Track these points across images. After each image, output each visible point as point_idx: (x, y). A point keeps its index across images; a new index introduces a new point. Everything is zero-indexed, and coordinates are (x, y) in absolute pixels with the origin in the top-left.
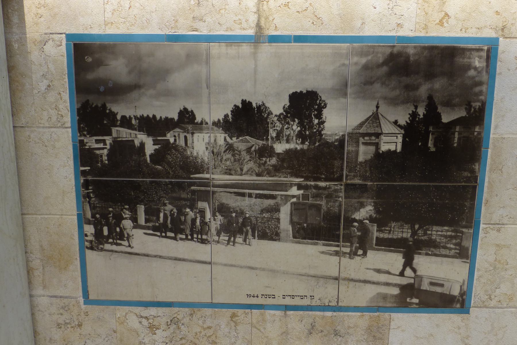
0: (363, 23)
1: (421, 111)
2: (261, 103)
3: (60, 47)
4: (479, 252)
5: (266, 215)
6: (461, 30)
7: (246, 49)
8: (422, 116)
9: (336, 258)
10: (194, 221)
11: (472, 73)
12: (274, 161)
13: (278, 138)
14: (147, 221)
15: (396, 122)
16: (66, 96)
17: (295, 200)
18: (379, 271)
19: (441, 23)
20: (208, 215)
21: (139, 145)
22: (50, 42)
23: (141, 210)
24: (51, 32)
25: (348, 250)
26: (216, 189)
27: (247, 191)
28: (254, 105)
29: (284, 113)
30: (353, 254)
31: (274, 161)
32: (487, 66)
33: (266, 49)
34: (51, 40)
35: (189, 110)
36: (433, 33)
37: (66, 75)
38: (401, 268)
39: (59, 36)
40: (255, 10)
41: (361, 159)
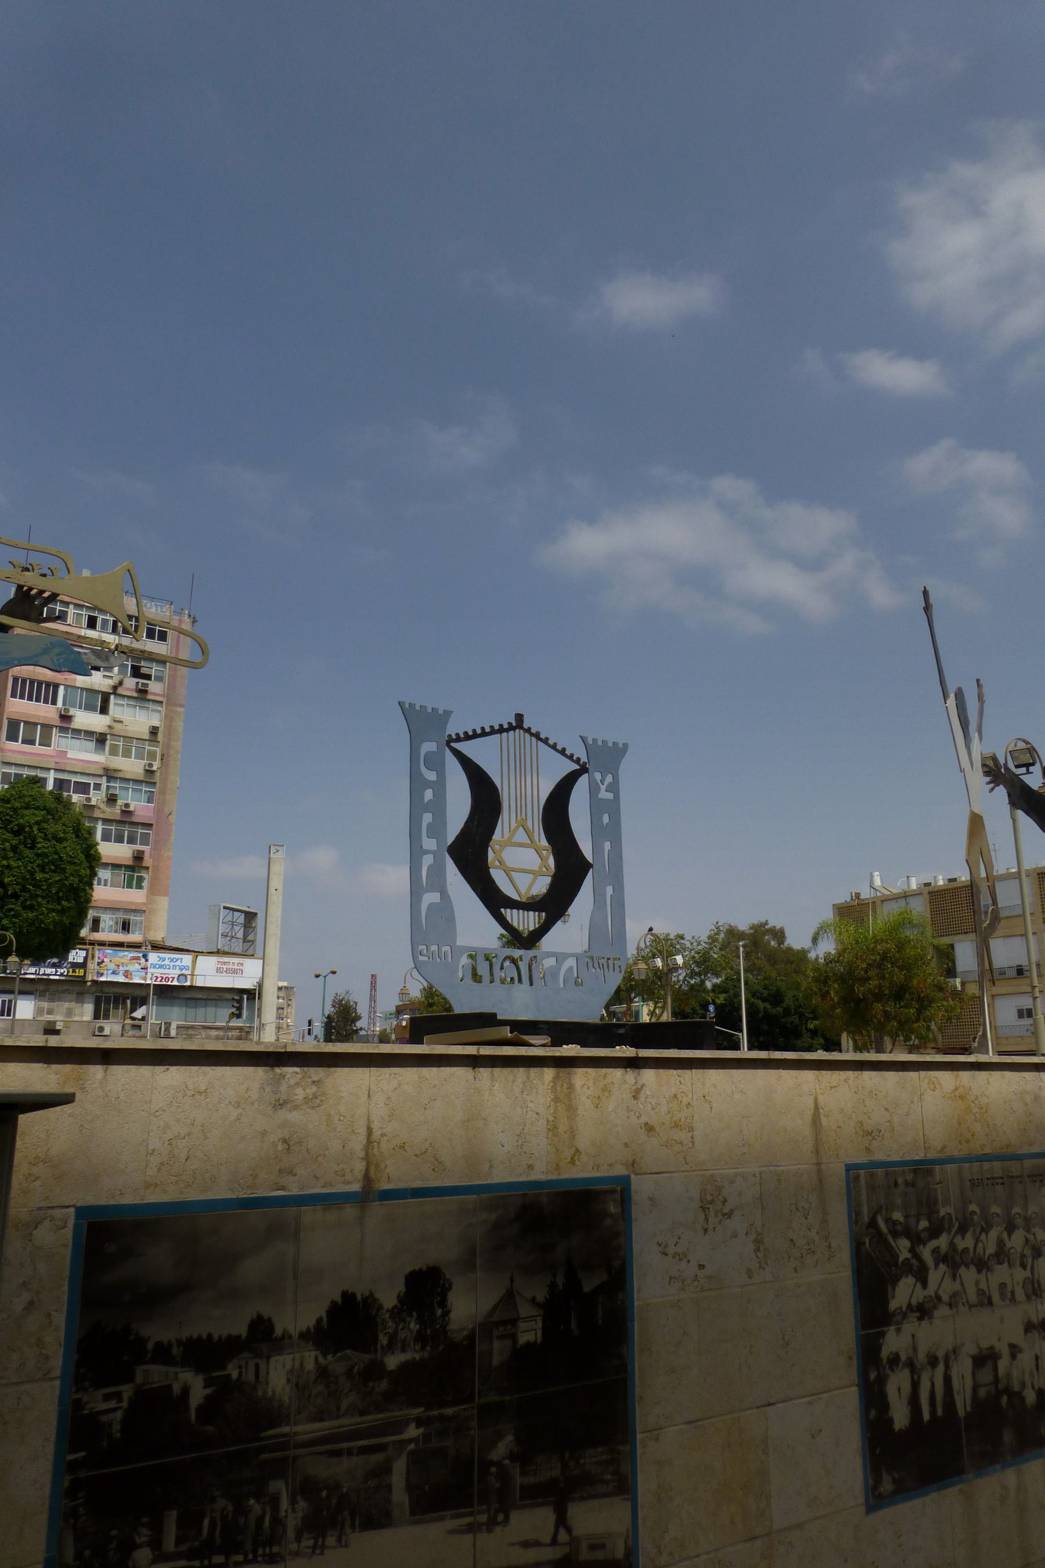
0: (491, 1167)
1: (560, 1280)
2: (367, 1294)
3: (62, 1231)
4: (640, 1479)
5: (371, 1483)
6: (593, 1168)
7: (350, 1212)
8: (561, 1287)
9: (468, 1538)
10: (260, 1520)
11: (608, 1222)
12: (384, 1385)
13: (390, 1347)
14: (179, 1541)
15: (533, 1300)
16: (60, 1319)
17: (412, 1446)
18: (526, 1544)
19: (572, 1162)
20: (284, 1504)
21: (179, 1391)
22: (47, 1223)
23: (172, 1517)
24: (50, 1205)
25: (483, 1518)
26: (298, 1451)
27: (345, 1445)
28: (359, 1298)
29: (399, 1304)
30: (491, 1525)
31: (384, 1385)
32: (623, 1210)
33: (377, 1210)
34: (49, 1219)
35: (265, 1318)
36: (565, 1176)
37: (67, 1280)
38: (552, 1530)
39: (64, 1211)
40: (362, 1154)
41: (496, 1361)
